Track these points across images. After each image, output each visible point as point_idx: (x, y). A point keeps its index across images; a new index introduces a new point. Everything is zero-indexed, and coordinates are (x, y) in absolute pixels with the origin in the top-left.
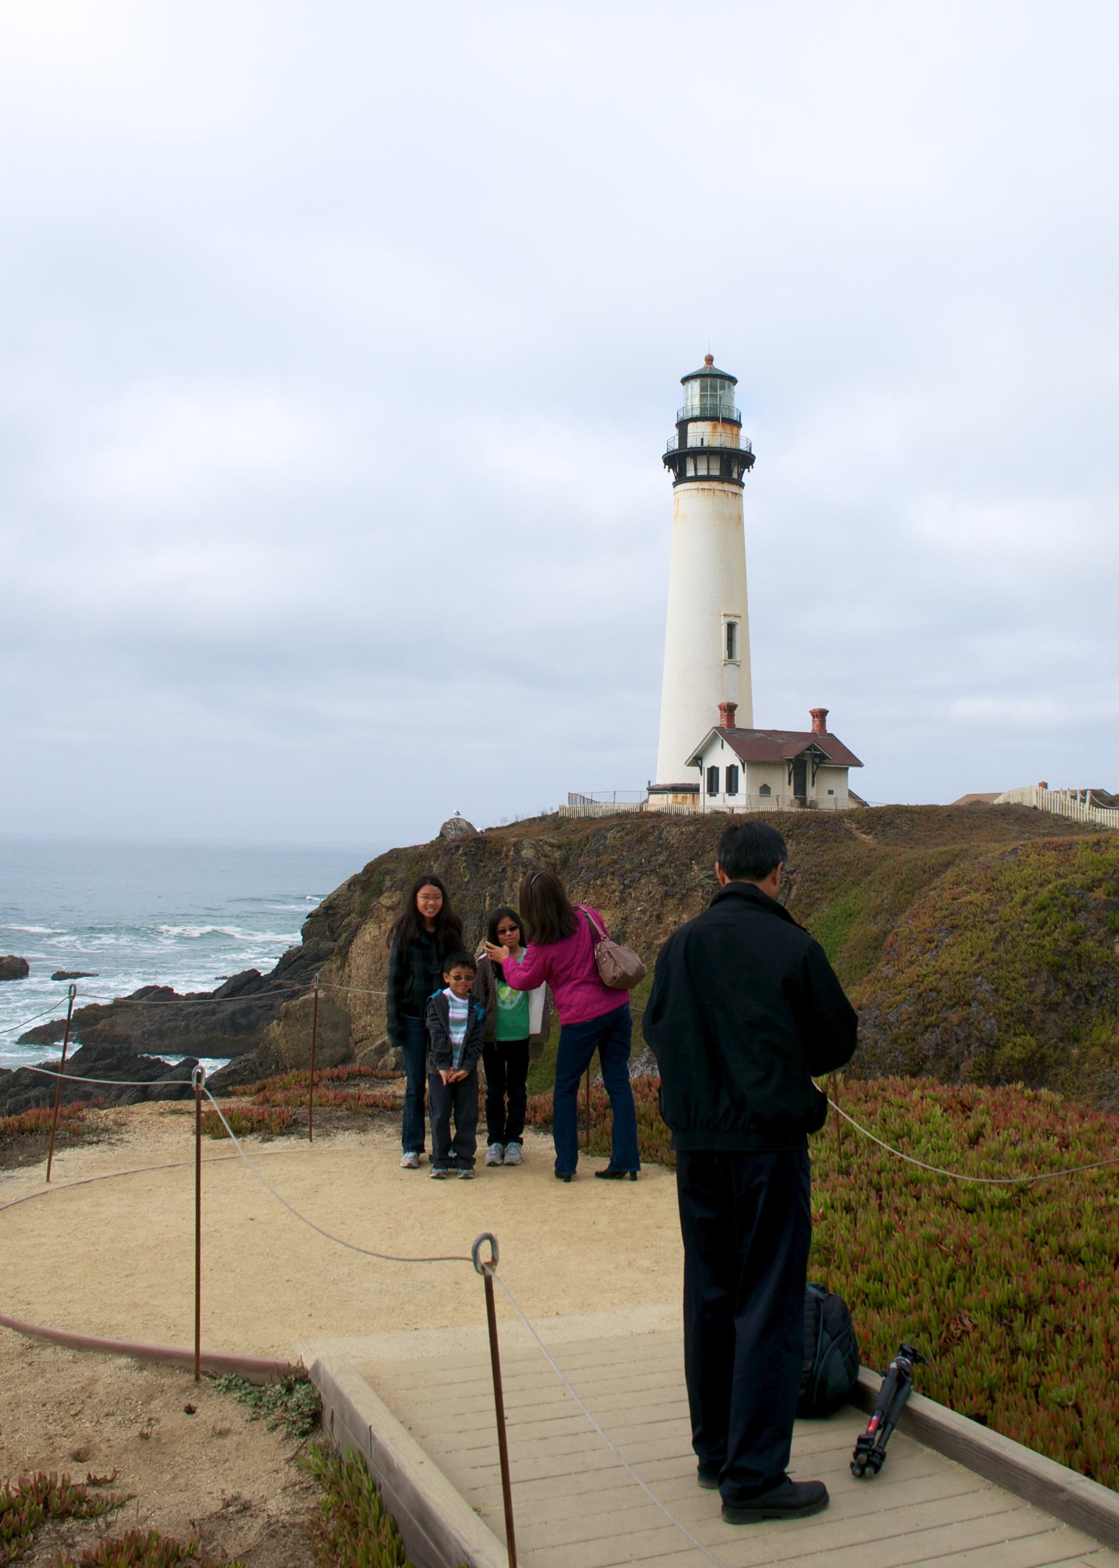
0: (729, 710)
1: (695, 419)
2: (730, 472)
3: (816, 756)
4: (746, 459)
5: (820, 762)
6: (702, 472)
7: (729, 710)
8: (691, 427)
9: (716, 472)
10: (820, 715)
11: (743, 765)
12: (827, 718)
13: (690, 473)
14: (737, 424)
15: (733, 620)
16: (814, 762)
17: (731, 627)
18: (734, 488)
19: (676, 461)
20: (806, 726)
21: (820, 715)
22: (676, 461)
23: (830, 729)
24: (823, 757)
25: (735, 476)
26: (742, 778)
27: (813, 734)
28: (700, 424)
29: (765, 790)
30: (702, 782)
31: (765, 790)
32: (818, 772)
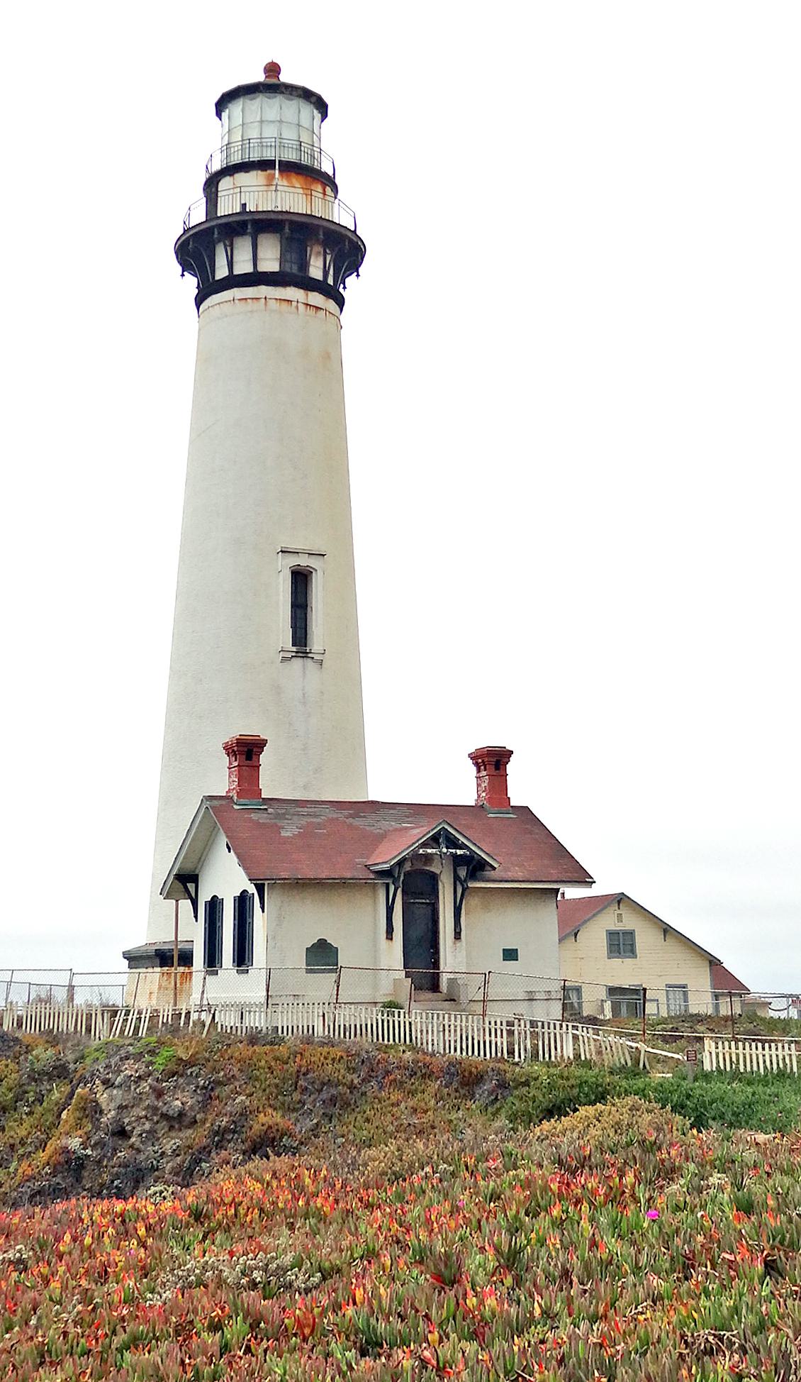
0: (247, 752)
1: (230, 170)
2: (304, 266)
3: (457, 861)
4: (347, 251)
5: (473, 875)
6: (243, 266)
7: (247, 752)
8: (225, 183)
9: (270, 261)
10: (493, 762)
11: (260, 889)
12: (511, 768)
13: (221, 272)
14: (329, 182)
15: (303, 561)
16: (456, 878)
17: (301, 579)
18: (316, 298)
19: (195, 251)
20: (463, 788)
21: (493, 762)
22: (195, 251)
23: (517, 797)
24: (474, 867)
25: (316, 272)
26: (260, 922)
27: (478, 809)
28: (242, 178)
29: (322, 955)
30: (195, 934)
31: (322, 955)
32: (470, 904)
